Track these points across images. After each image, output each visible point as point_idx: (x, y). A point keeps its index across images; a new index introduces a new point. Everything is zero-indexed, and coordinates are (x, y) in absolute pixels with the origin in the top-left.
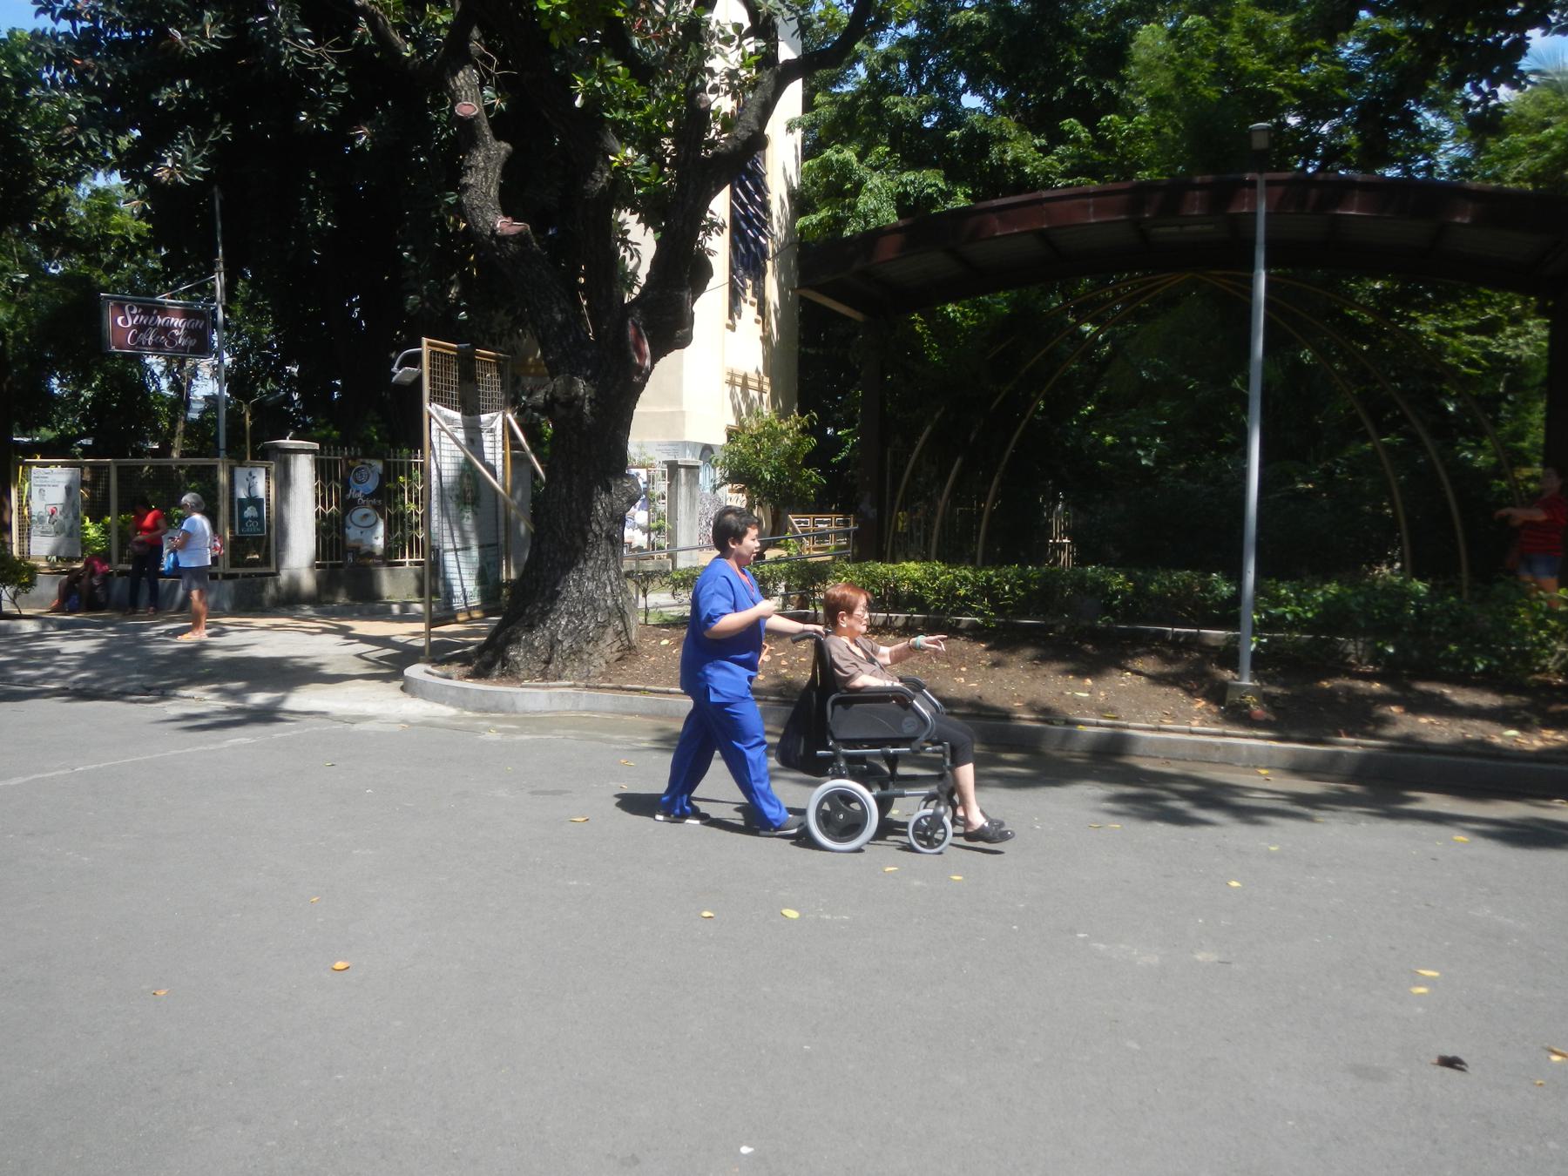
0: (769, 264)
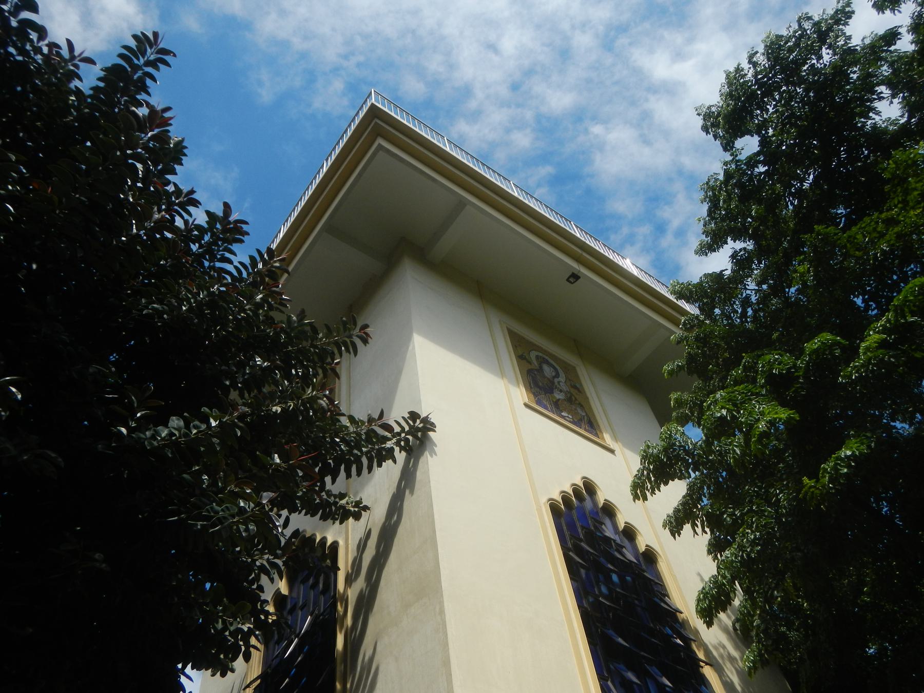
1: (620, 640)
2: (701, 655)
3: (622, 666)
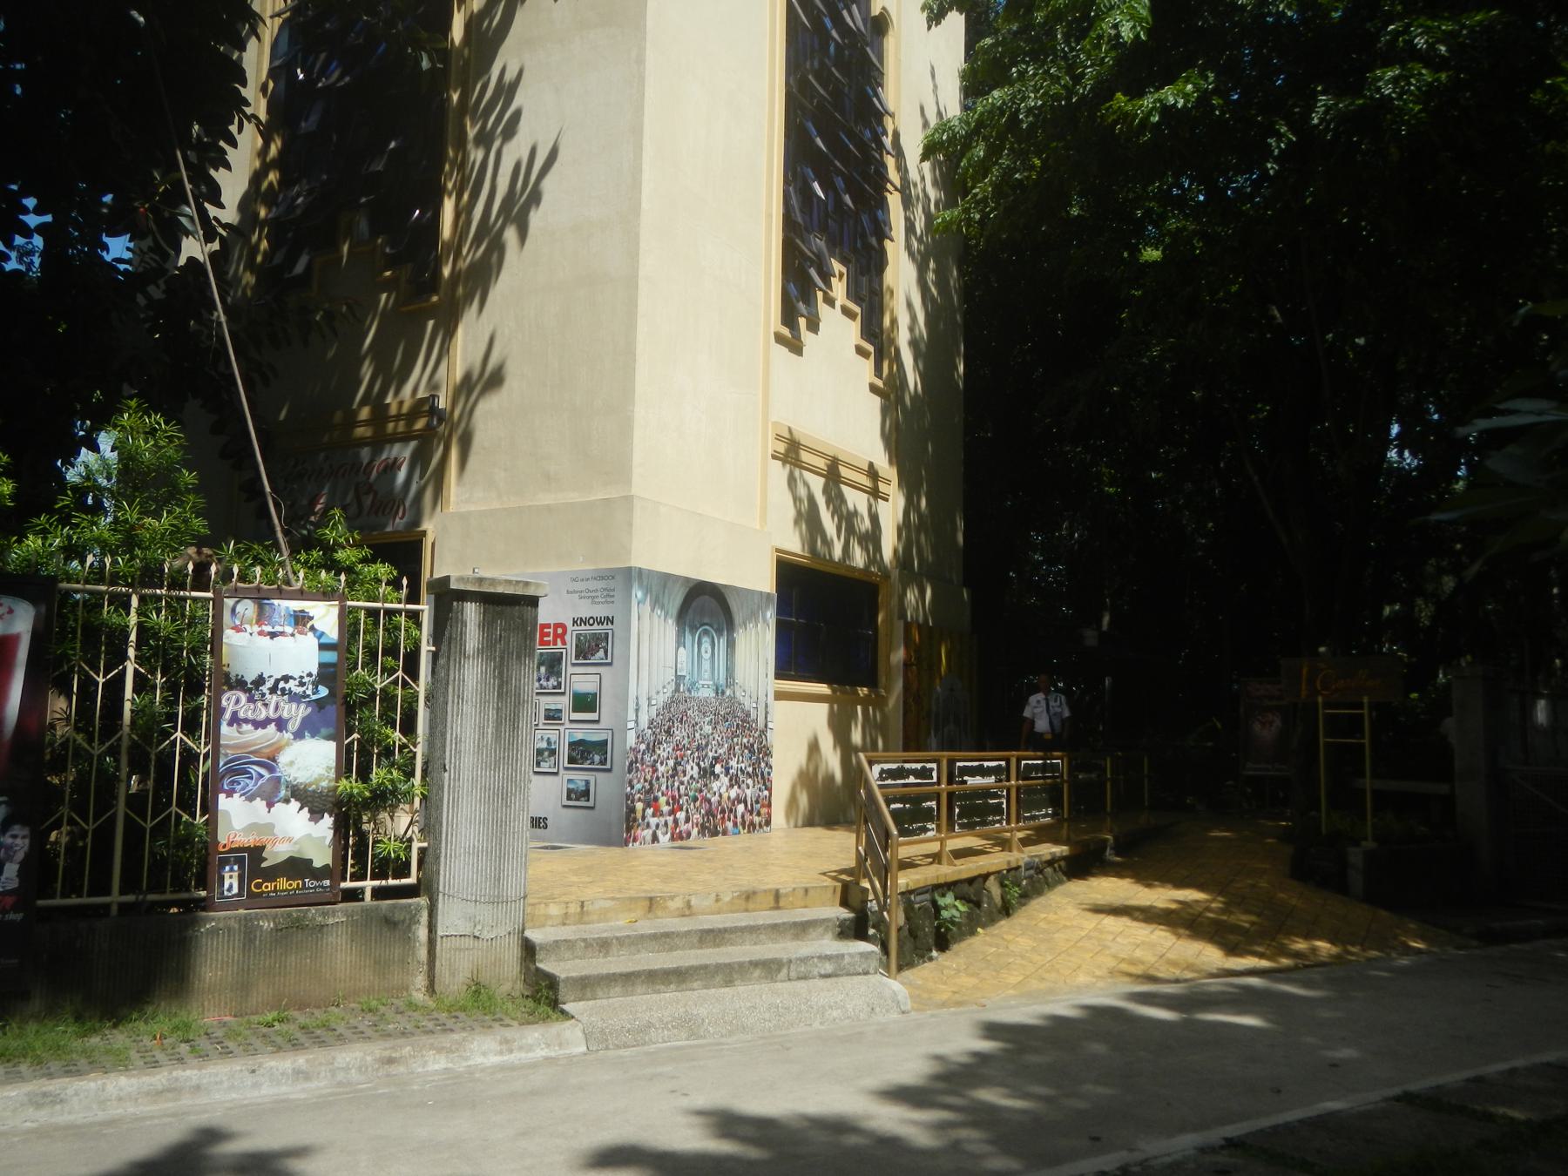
1: (819, 141)
2: (893, 175)
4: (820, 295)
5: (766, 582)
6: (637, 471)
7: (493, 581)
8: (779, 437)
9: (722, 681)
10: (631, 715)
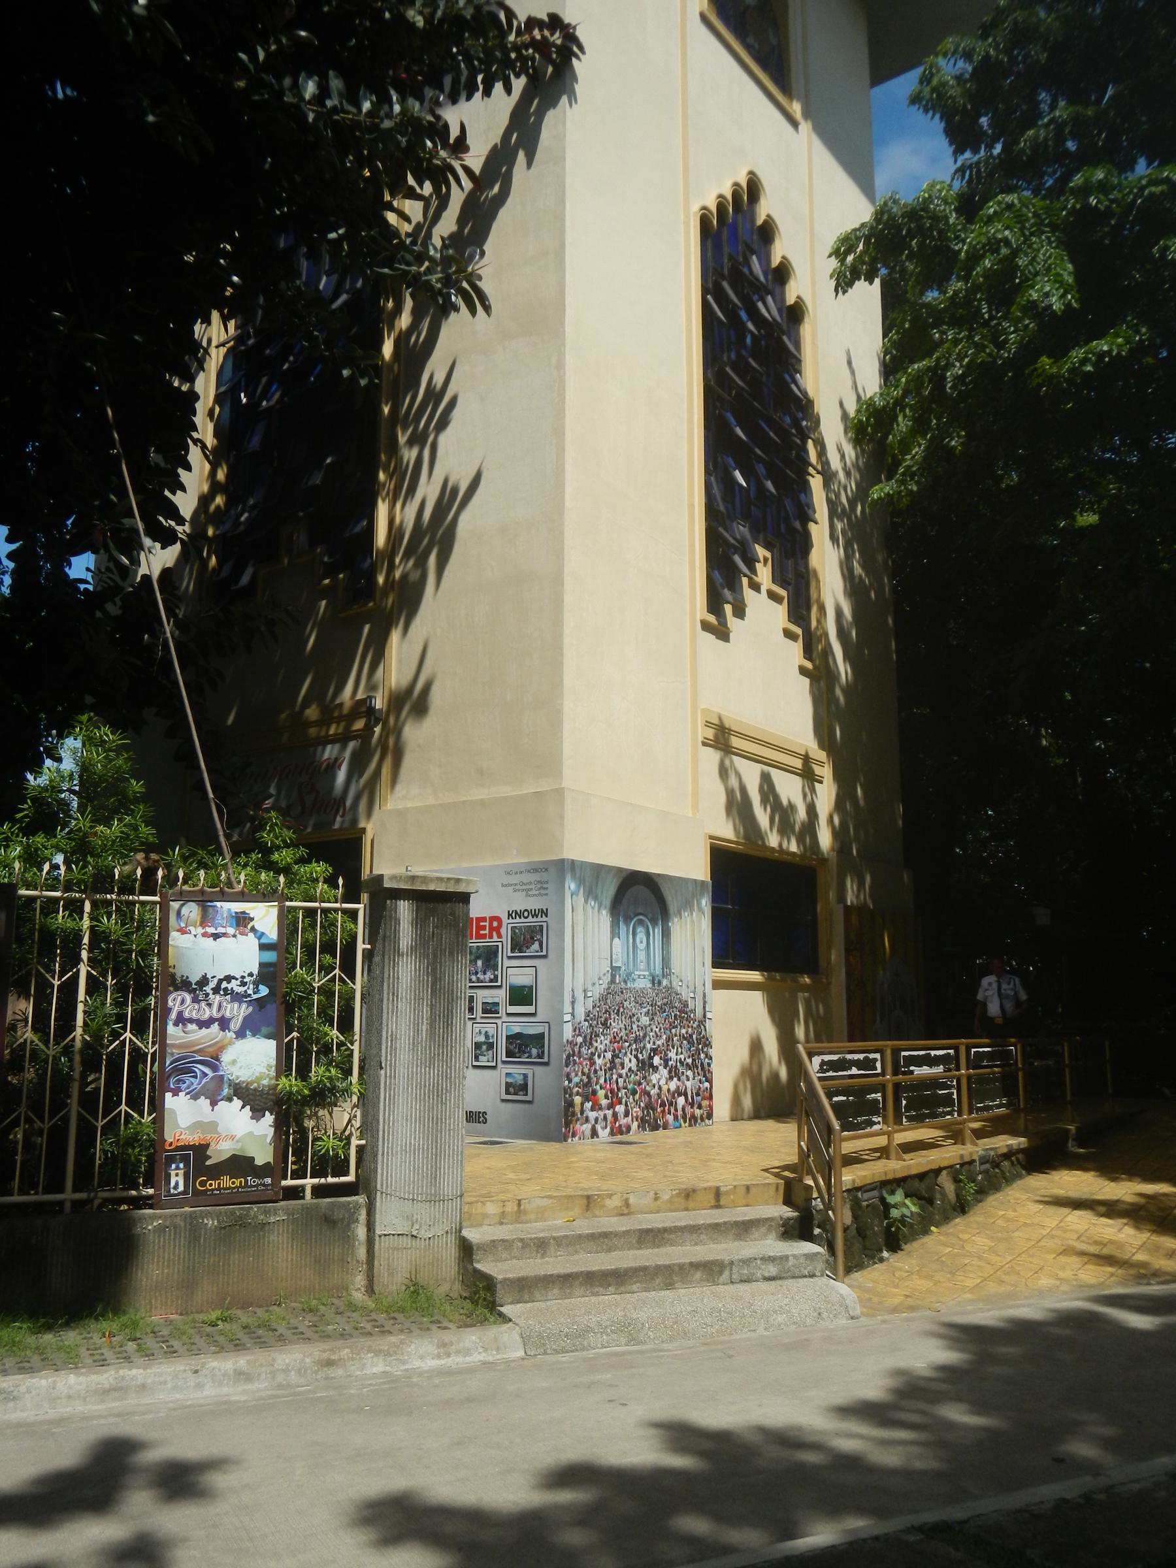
0: (819, 531)
1: (739, 431)
3: (731, 461)
4: (745, 581)
5: (698, 869)
6: (567, 763)
7: (425, 879)
8: (708, 724)
9: (658, 971)
10: (567, 1008)
